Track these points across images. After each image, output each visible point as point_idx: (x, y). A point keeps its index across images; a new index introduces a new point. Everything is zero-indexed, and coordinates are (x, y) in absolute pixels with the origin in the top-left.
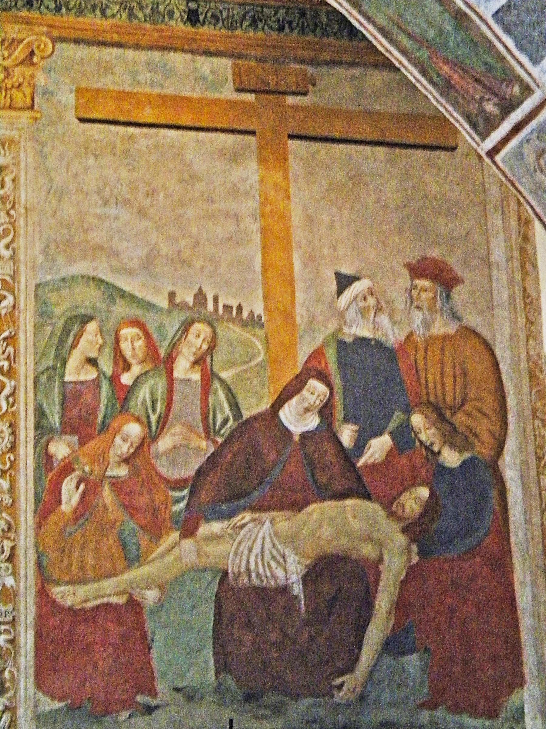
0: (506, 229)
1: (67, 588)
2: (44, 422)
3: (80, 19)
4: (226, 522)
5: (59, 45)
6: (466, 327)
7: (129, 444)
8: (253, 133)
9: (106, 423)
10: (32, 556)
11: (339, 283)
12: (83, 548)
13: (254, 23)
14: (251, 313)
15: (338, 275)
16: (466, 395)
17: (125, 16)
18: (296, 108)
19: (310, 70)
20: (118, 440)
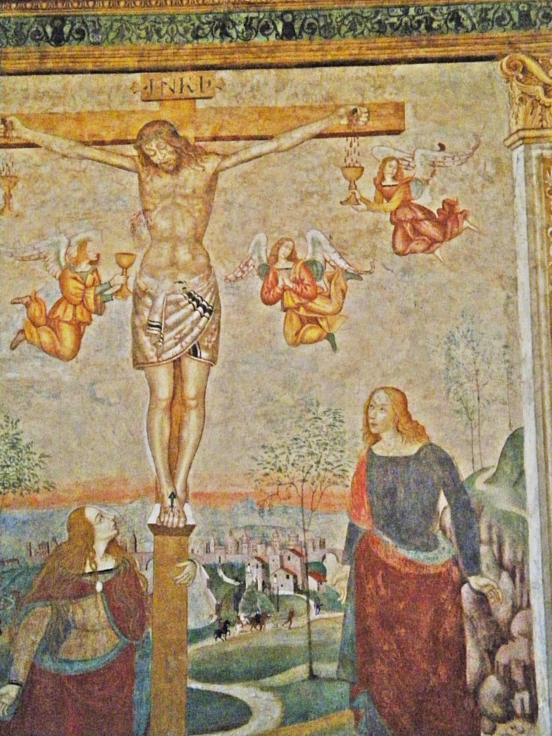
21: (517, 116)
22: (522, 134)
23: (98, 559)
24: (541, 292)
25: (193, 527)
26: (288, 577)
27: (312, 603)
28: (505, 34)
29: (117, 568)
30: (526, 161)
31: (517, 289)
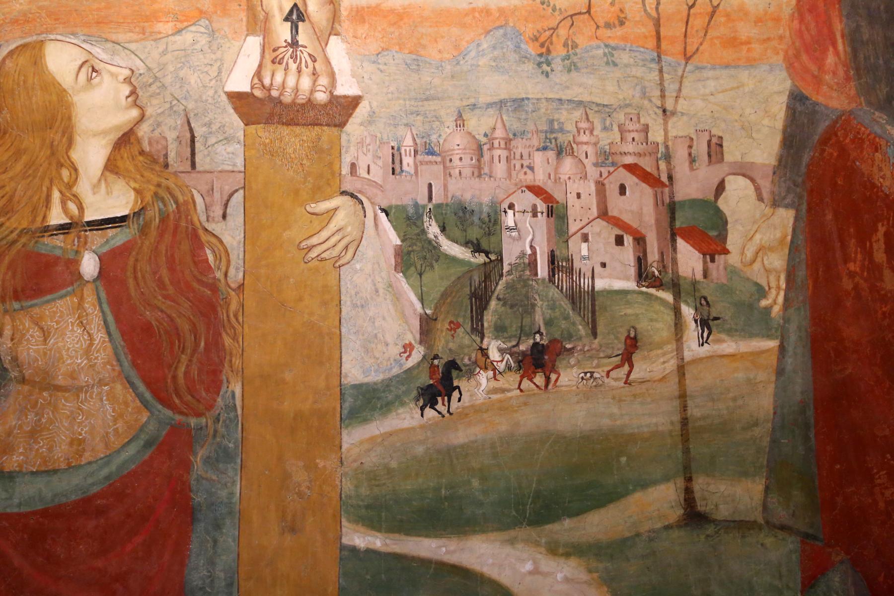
23: (83, 188)
25: (354, 102)
26: (619, 241)
27: (688, 312)
29: (137, 214)
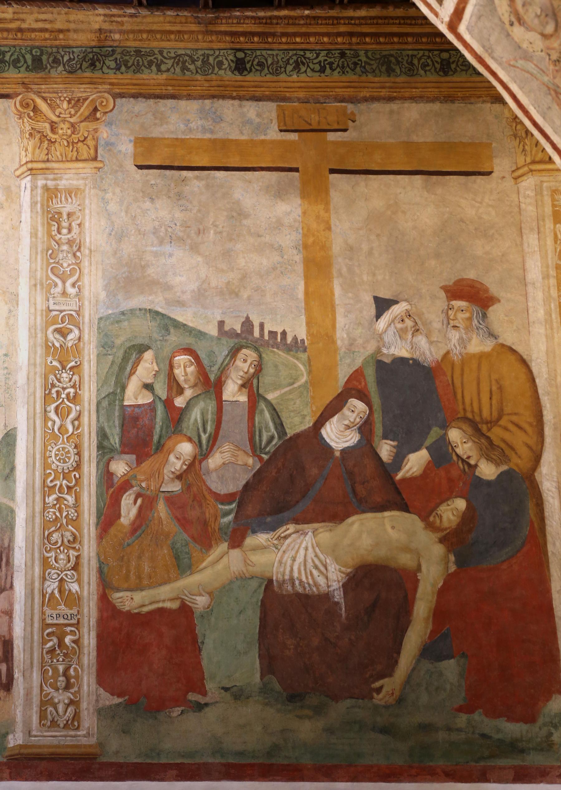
0: (542, 248)
1: (128, 594)
2: (105, 443)
3: (139, 75)
4: (272, 533)
5: (118, 101)
6: (503, 345)
7: (182, 461)
8: (296, 170)
9: (162, 443)
10: (94, 563)
11: (377, 308)
12: (139, 557)
13: (297, 67)
14: (295, 338)
15: (377, 300)
16: (502, 410)
17: (178, 70)
18: (335, 143)
19: (350, 107)
20: (172, 458)
21: (27, 150)
22: (30, 166)
24: (39, 307)
28: (20, 75)
30: (32, 190)
31: (18, 304)
